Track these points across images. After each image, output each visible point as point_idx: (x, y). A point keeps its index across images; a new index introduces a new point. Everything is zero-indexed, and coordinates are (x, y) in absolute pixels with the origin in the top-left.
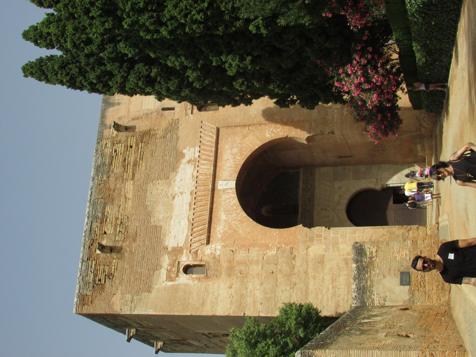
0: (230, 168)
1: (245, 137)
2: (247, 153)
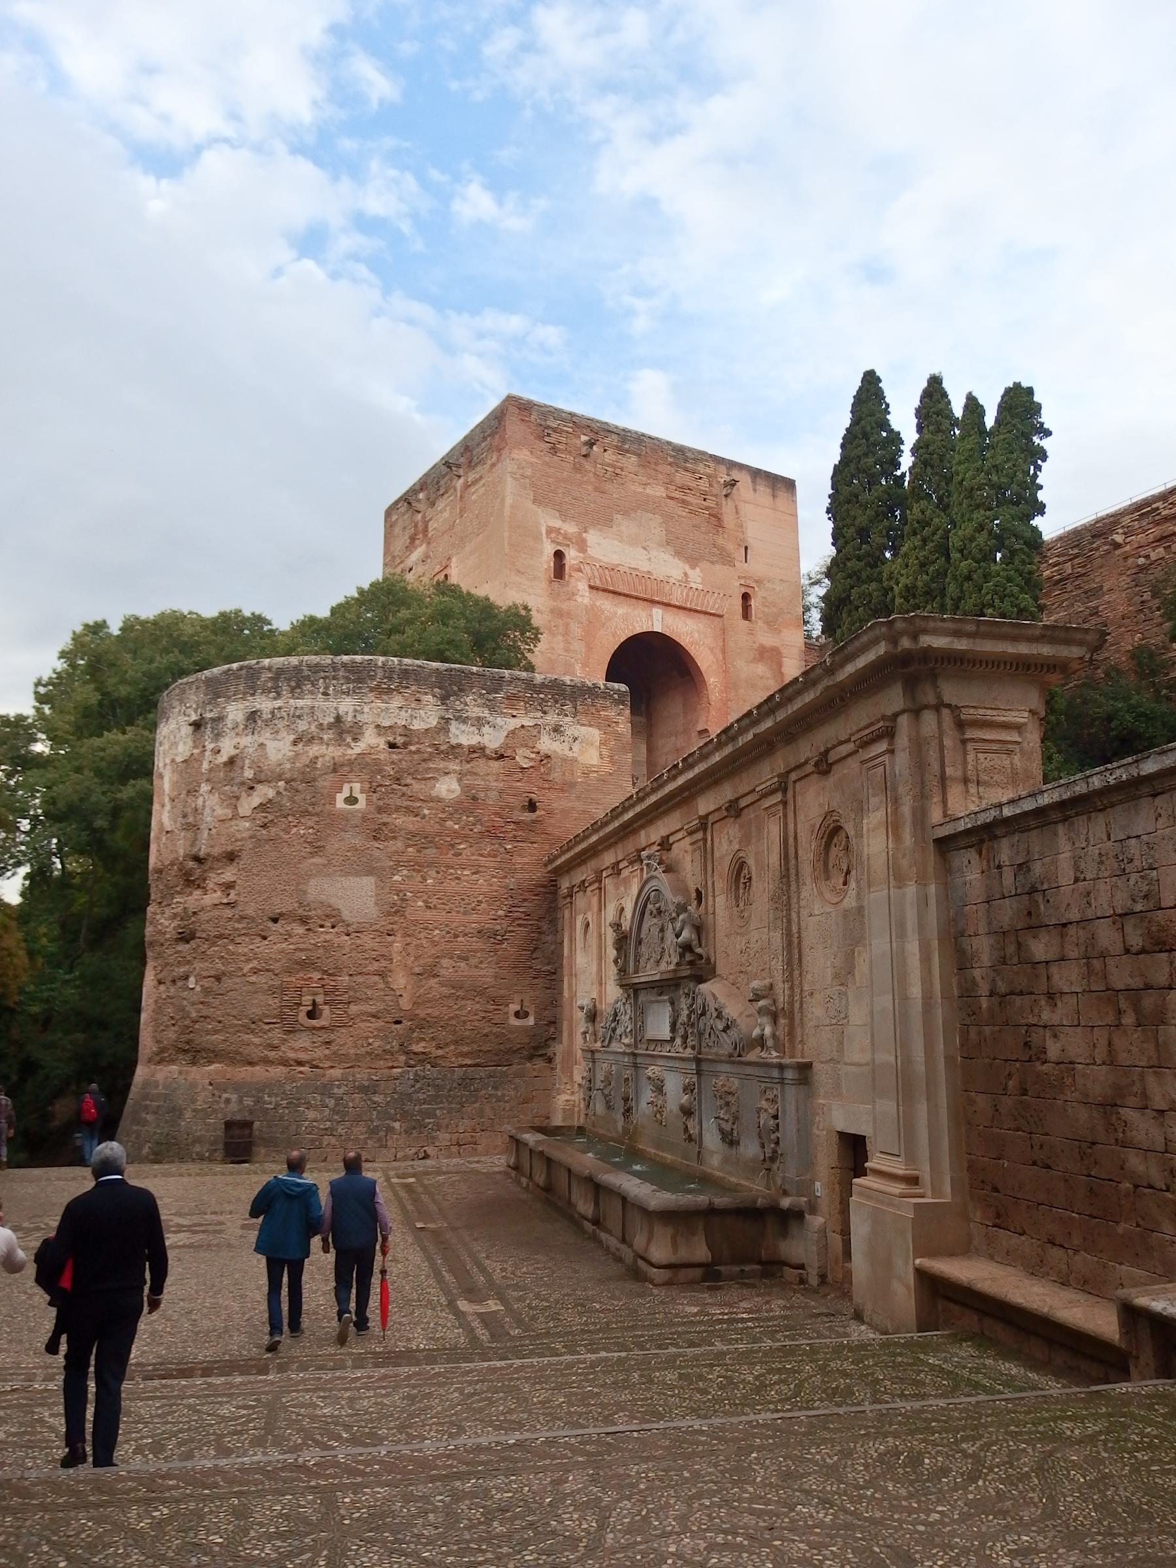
1: (712, 650)
2: (692, 651)
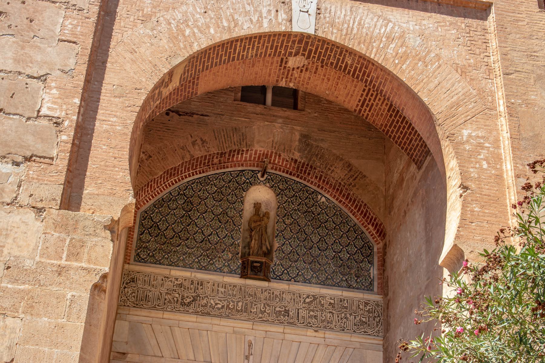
0: (359, 24)
